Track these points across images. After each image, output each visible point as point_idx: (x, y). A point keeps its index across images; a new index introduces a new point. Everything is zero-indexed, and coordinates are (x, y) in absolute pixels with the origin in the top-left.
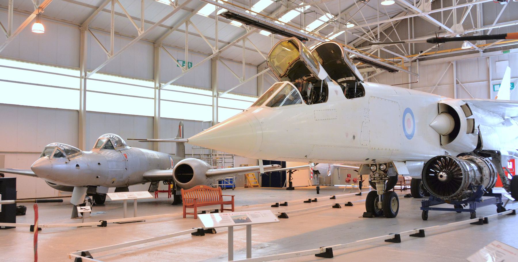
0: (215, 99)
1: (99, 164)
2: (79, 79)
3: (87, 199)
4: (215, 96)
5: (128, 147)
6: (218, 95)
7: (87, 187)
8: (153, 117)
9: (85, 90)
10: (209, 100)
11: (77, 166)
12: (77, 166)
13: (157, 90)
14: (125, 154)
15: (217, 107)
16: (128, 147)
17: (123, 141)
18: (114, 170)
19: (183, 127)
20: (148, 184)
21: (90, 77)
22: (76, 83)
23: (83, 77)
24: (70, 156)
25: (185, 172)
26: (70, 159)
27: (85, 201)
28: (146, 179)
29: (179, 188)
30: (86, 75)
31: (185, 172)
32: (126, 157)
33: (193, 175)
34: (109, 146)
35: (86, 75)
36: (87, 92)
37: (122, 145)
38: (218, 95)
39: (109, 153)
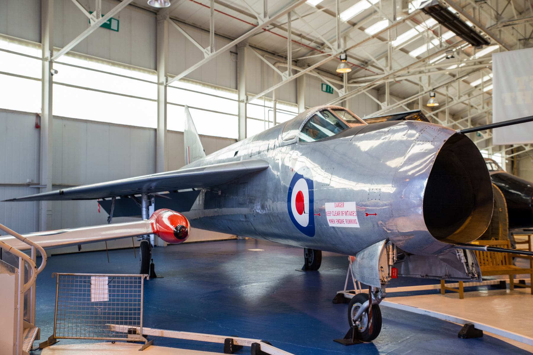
0: (243, 105)
2: (41, 61)
4: (243, 101)
6: (247, 100)
8: (155, 130)
9: (51, 82)
10: (233, 107)
13: (162, 88)
15: (246, 118)
21: (57, 60)
22: (35, 68)
23: (46, 59)
30: (52, 55)
35: (52, 55)
36: (54, 85)
38: (247, 100)
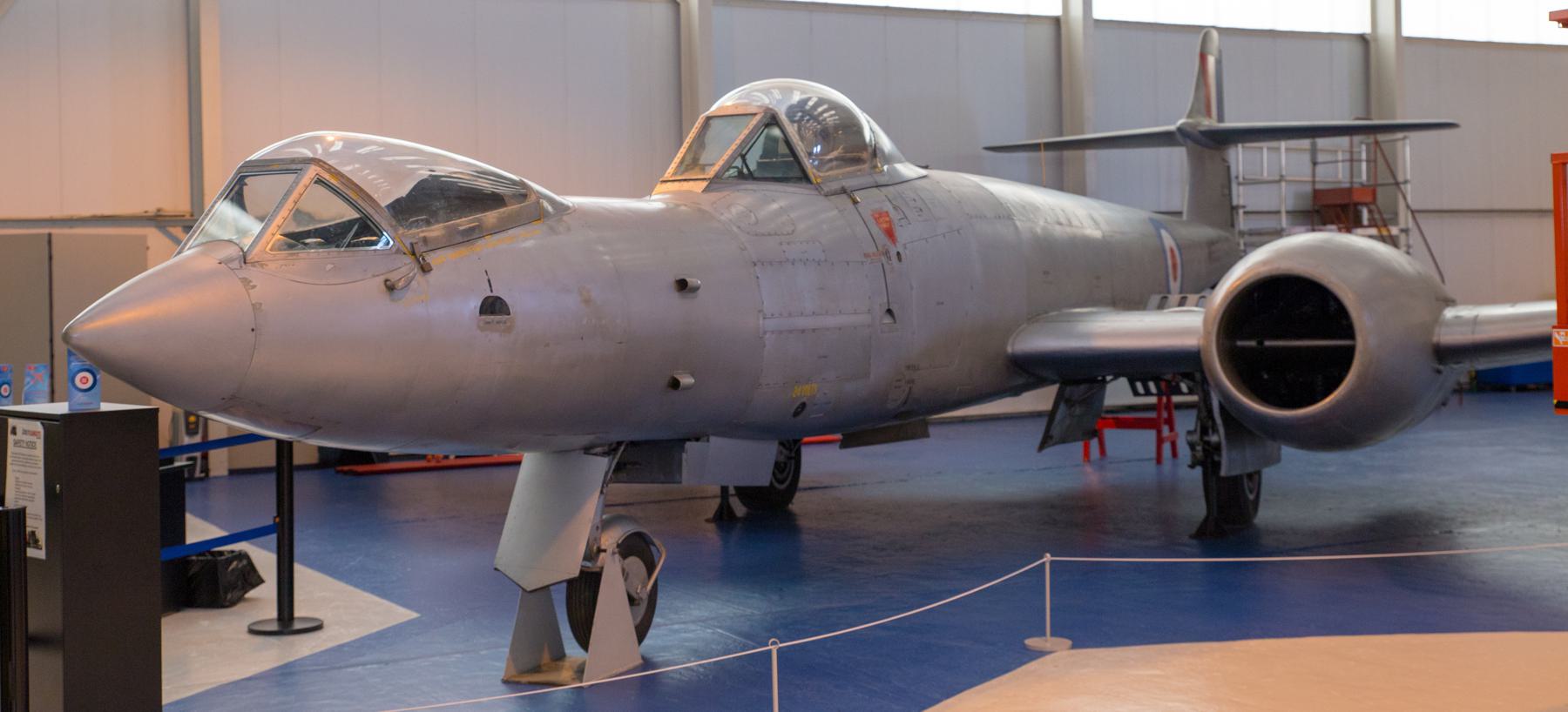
1: (682, 285)
3: (611, 539)
5: (908, 170)
7: (611, 451)
8: (1057, 21)
11: (493, 306)
12: (493, 306)
14: (880, 216)
16: (908, 170)
17: (871, 129)
18: (802, 322)
19: (1219, 62)
20: (1040, 399)
24: (436, 231)
25: (1290, 332)
26: (431, 259)
27: (593, 553)
28: (1029, 371)
29: (1239, 425)
31: (1290, 332)
32: (890, 233)
33: (1350, 351)
34: (776, 158)
37: (859, 153)
39: (779, 203)
